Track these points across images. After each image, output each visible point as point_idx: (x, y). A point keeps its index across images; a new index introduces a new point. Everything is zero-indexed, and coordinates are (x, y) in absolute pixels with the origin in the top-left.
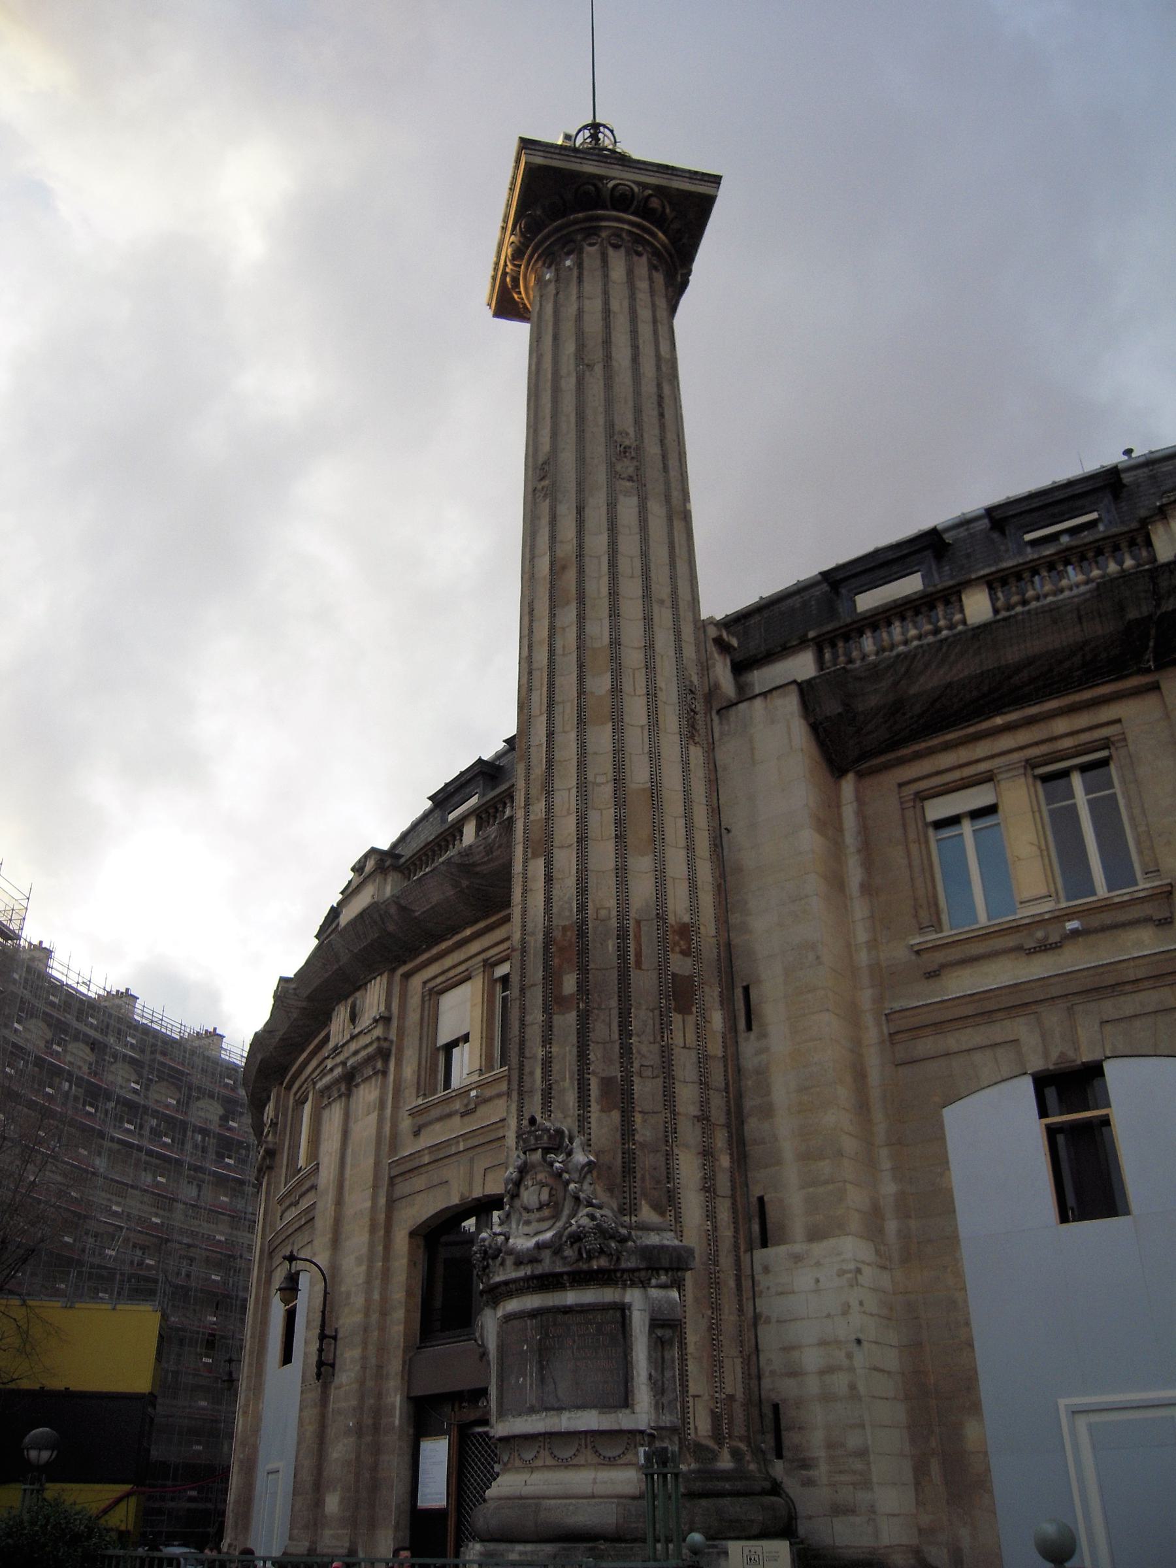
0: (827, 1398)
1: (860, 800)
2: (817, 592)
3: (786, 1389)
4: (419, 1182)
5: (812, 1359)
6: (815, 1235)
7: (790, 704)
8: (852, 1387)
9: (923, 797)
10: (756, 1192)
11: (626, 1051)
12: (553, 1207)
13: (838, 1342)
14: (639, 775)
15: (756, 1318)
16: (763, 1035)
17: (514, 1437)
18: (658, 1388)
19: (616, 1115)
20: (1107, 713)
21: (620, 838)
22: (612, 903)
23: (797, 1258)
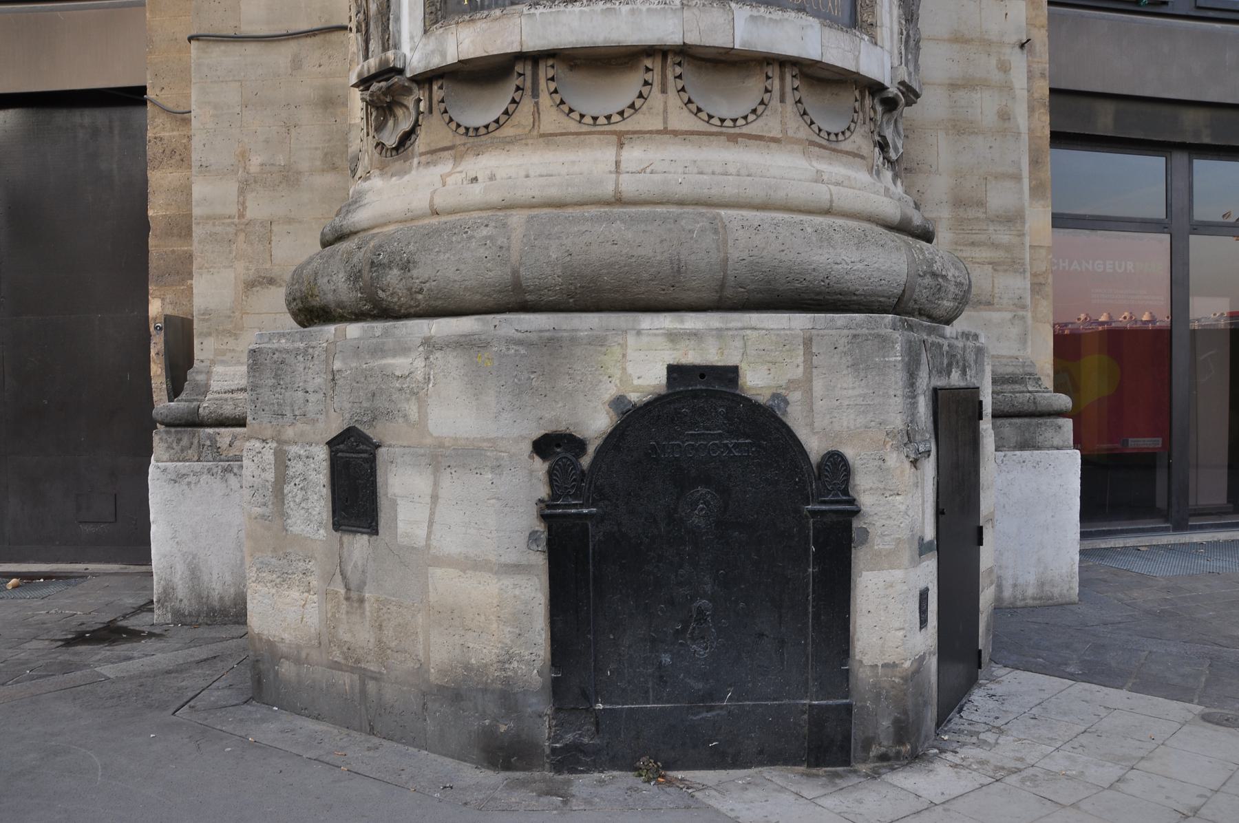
0: (960, 128)
8: (1005, 116)
13: (986, 44)
17: (535, 58)
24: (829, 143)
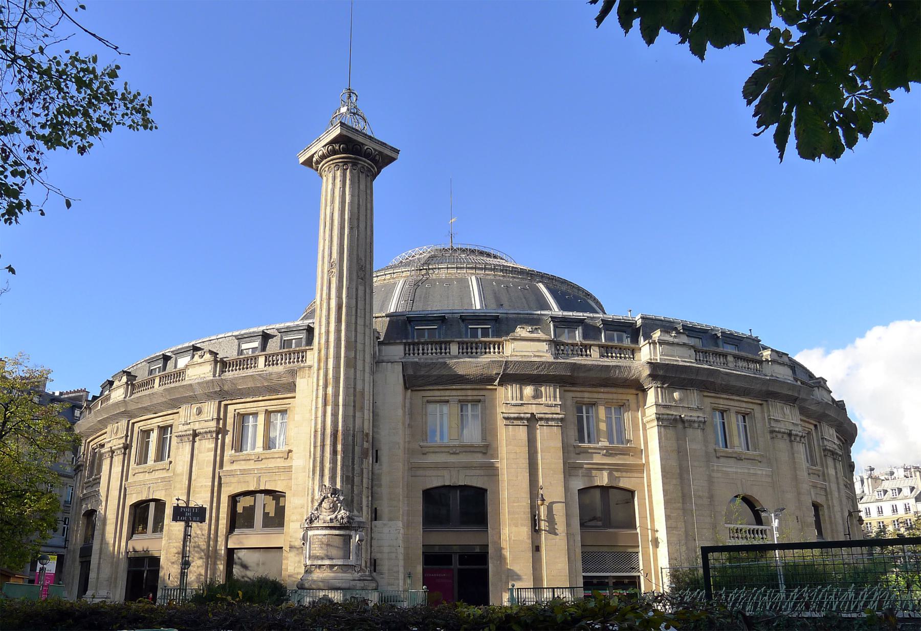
0: (390, 559)
1: (411, 399)
2: (402, 318)
3: (378, 556)
4: (234, 480)
5: (386, 550)
6: (390, 520)
7: (399, 368)
9: (428, 402)
10: (375, 506)
11: (353, 469)
12: (334, 509)
14: (359, 387)
15: (372, 538)
16: (381, 465)
18: (357, 555)
19: (350, 486)
20: (482, 393)
21: (354, 406)
22: (351, 426)
23: (385, 525)
24: (345, 572)
